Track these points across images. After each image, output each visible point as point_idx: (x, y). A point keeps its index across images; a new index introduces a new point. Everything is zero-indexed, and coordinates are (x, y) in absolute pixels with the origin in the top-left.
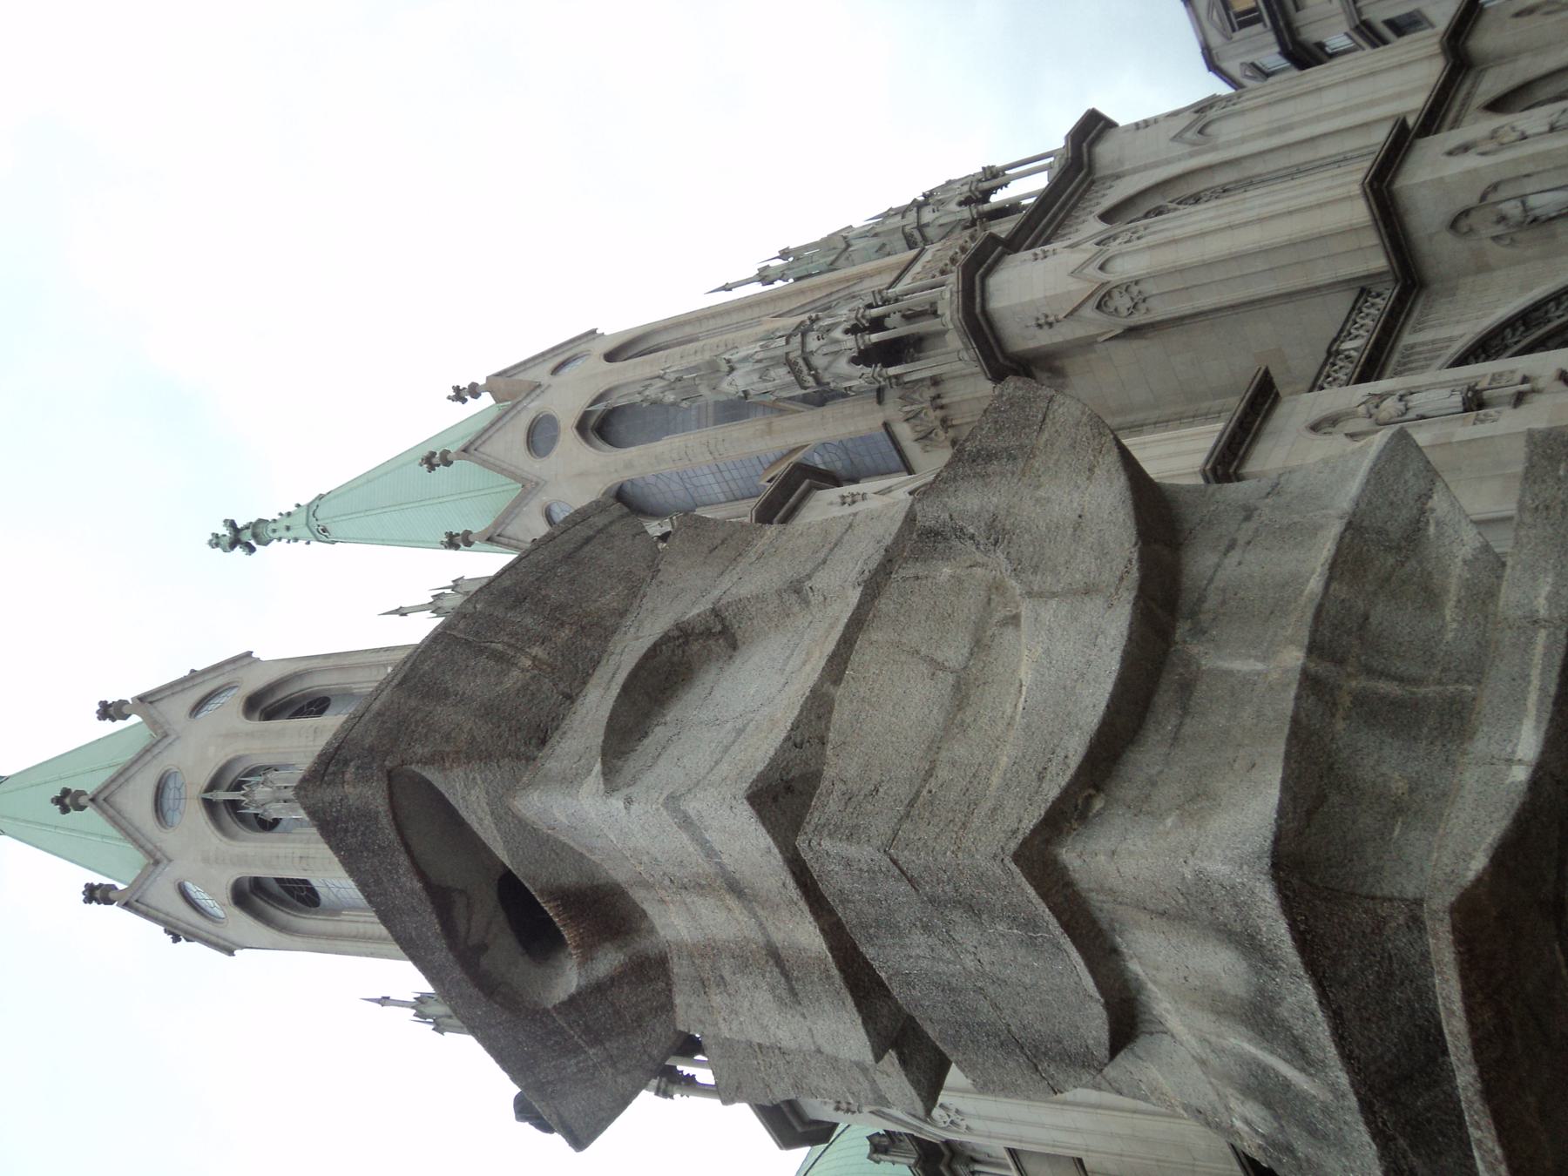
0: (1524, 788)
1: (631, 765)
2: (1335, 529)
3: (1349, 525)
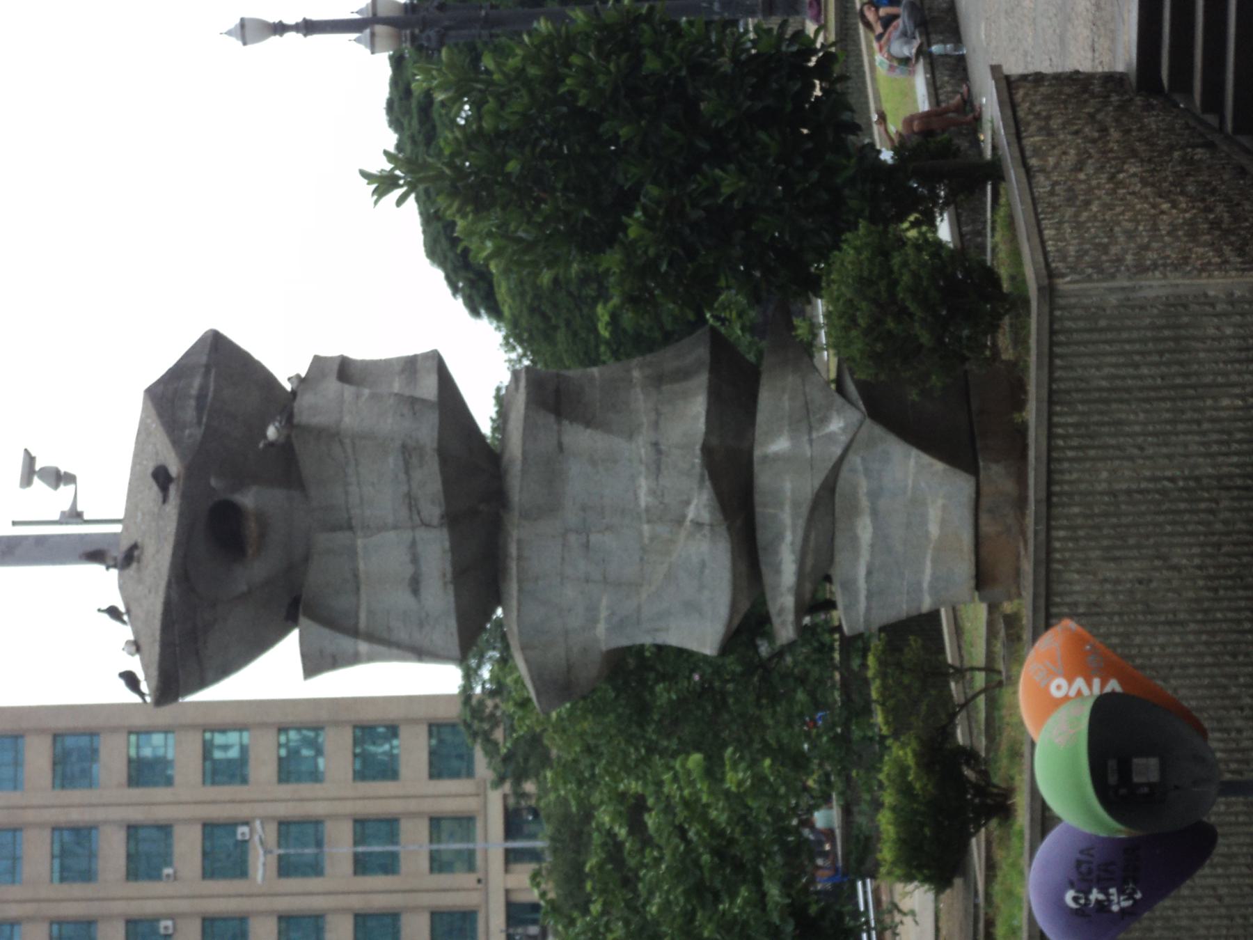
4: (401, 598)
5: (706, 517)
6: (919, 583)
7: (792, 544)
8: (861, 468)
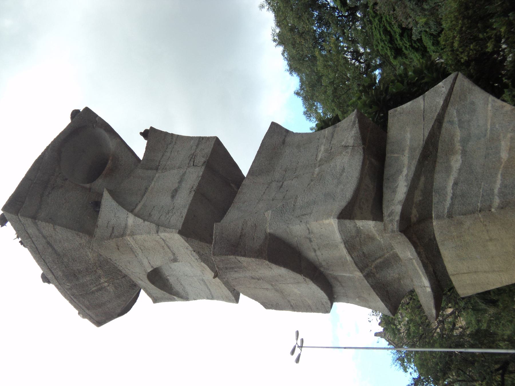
0: (431, 292)
1: (177, 287)
2: (342, 246)
3: (345, 244)
4: (165, 200)
5: (351, 142)
6: (492, 190)
7: (407, 175)
8: (456, 119)
